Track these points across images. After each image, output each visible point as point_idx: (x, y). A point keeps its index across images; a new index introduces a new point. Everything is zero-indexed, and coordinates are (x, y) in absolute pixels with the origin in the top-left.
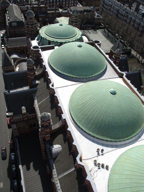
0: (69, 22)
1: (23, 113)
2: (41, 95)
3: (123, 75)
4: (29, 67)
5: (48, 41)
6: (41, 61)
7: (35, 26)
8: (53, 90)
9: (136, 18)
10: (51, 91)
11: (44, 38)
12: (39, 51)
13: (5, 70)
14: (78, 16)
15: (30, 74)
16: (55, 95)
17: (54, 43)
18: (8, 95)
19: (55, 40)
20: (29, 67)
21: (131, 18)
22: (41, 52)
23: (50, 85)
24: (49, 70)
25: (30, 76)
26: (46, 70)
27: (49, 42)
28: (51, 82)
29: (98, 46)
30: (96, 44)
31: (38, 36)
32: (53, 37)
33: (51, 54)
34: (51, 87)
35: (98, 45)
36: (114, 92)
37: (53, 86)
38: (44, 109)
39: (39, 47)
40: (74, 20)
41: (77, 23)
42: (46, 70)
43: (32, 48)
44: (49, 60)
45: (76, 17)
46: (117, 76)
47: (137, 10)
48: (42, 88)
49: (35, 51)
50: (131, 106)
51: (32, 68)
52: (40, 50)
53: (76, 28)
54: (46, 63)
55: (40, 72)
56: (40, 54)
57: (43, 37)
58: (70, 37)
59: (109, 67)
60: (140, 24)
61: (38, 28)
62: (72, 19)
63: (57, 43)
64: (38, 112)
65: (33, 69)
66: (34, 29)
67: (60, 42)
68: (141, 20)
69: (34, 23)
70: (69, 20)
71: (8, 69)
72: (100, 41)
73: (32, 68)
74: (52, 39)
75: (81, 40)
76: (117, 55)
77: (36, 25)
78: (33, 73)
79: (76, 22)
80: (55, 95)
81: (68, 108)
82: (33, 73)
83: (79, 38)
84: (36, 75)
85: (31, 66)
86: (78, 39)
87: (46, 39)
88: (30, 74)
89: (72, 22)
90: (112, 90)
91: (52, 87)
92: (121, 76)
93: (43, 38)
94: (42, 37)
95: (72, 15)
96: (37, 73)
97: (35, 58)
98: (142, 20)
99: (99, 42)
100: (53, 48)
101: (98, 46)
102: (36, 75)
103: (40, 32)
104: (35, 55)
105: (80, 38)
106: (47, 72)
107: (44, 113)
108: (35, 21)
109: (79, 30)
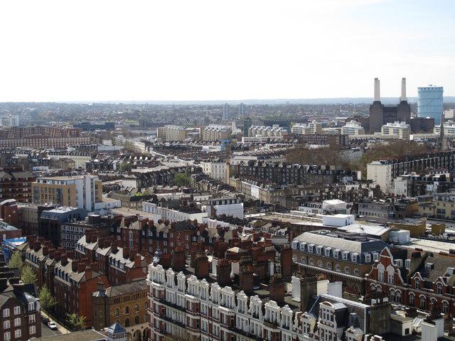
47: (311, 302)
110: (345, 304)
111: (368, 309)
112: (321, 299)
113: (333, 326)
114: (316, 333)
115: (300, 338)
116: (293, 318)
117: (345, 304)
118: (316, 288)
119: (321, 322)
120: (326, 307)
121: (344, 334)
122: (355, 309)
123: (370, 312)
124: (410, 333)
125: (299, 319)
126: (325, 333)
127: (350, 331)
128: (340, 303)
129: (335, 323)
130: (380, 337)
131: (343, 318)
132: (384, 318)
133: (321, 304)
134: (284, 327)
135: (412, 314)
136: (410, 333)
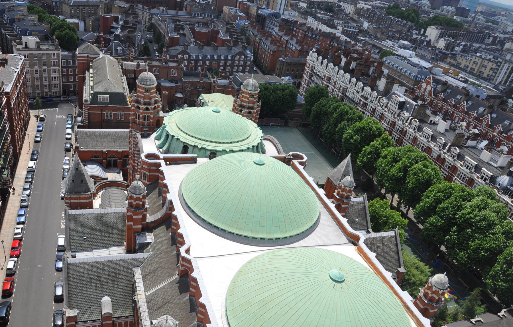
0: (234, 106)
1: (105, 314)
2: (154, 271)
3: (357, 238)
4: (133, 201)
5: (182, 145)
6: (164, 189)
7: (155, 108)
8: (189, 262)
9: (385, 111)
10: (182, 265)
11: (173, 136)
12: (159, 165)
13: (72, 201)
14: (256, 94)
15: (134, 217)
16: (193, 275)
17: (196, 150)
18: (73, 264)
19: (201, 144)
20: (133, 201)
21: (374, 110)
22: (164, 168)
23: (182, 250)
24: (179, 212)
25: (132, 223)
26: (174, 213)
27: (186, 149)
28: (183, 243)
29: (301, 168)
30: (296, 162)
31: (159, 130)
32: (200, 137)
33: (188, 175)
34: (183, 254)
35: (301, 164)
36: (341, 278)
37: (188, 251)
38: (159, 308)
39: (162, 156)
40: (246, 102)
41: (252, 111)
42: (174, 213)
43: (143, 156)
44: (183, 189)
45: (252, 96)
46: (344, 239)
47: (387, 93)
48: (159, 254)
49: (150, 165)
50: (379, 313)
51: (141, 203)
52: (163, 163)
53: (250, 121)
54: (173, 196)
55: (158, 215)
56: (162, 173)
57: (171, 133)
58: (236, 140)
59: (326, 218)
60: (393, 124)
61: (161, 114)
62: (242, 101)
63: (202, 151)
64: (142, 314)
65: (141, 207)
66: (151, 113)
67: (211, 150)
68: (396, 116)
69: (153, 101)
70: (235, 102)
71: (79, 201)
72: (304, 156)
73: (141, 203)
74: (191, 142)
75: (259, 149)
76: (344, 190)
77: (156, 105)
78: (141, 217)
79: (249, 108)
80: (193, 275)
81: (224, 309)
82: (141, 217)
83: (255, 144)
84: (147, 221)
85: (138, 199)
86: (253, 146)
87: (178, 139)
88: (134, 217)
89: (241, 106)
90: (335, 272)
91: (186, 255)
92: (354, 240)
93: (170, 137)
94: (168, 136)
95: (244, 92)
96: (150, 218)
97: (149, 181)
98: (399, 115)
99: (302, 158)
100: (194, 161)
101: (301, 168)
102: (147, 221)
103: (165, 121)
104: (148, 174)
105: (258, 144)
106: (176, 218)
107: (165, 316)
108: (155, 97)
109: (256, 125)
110: (405, 99)
111: (416, 105)
112: (394, 94)
113: (396, 108)
114: (386, 109)
115: (376, 109)
116: (377, 98)
117: (405, 99)
118: (393, 87)
119: (390, 104)
120: (395, 98)
121: (400, 113)
122: (409, 103)
123: (416, 107)
124: (432, 123)
125: (379, 99)
126: (390, 110)
127: (403, 113)
128: (402, 99)
129: (397, 107)
130: (418, 121)
131: (402, 106)
132: (422, 112)
133: (393, 96)
134: (370, 101)
135: (435, 113)
136: (432, 123)
